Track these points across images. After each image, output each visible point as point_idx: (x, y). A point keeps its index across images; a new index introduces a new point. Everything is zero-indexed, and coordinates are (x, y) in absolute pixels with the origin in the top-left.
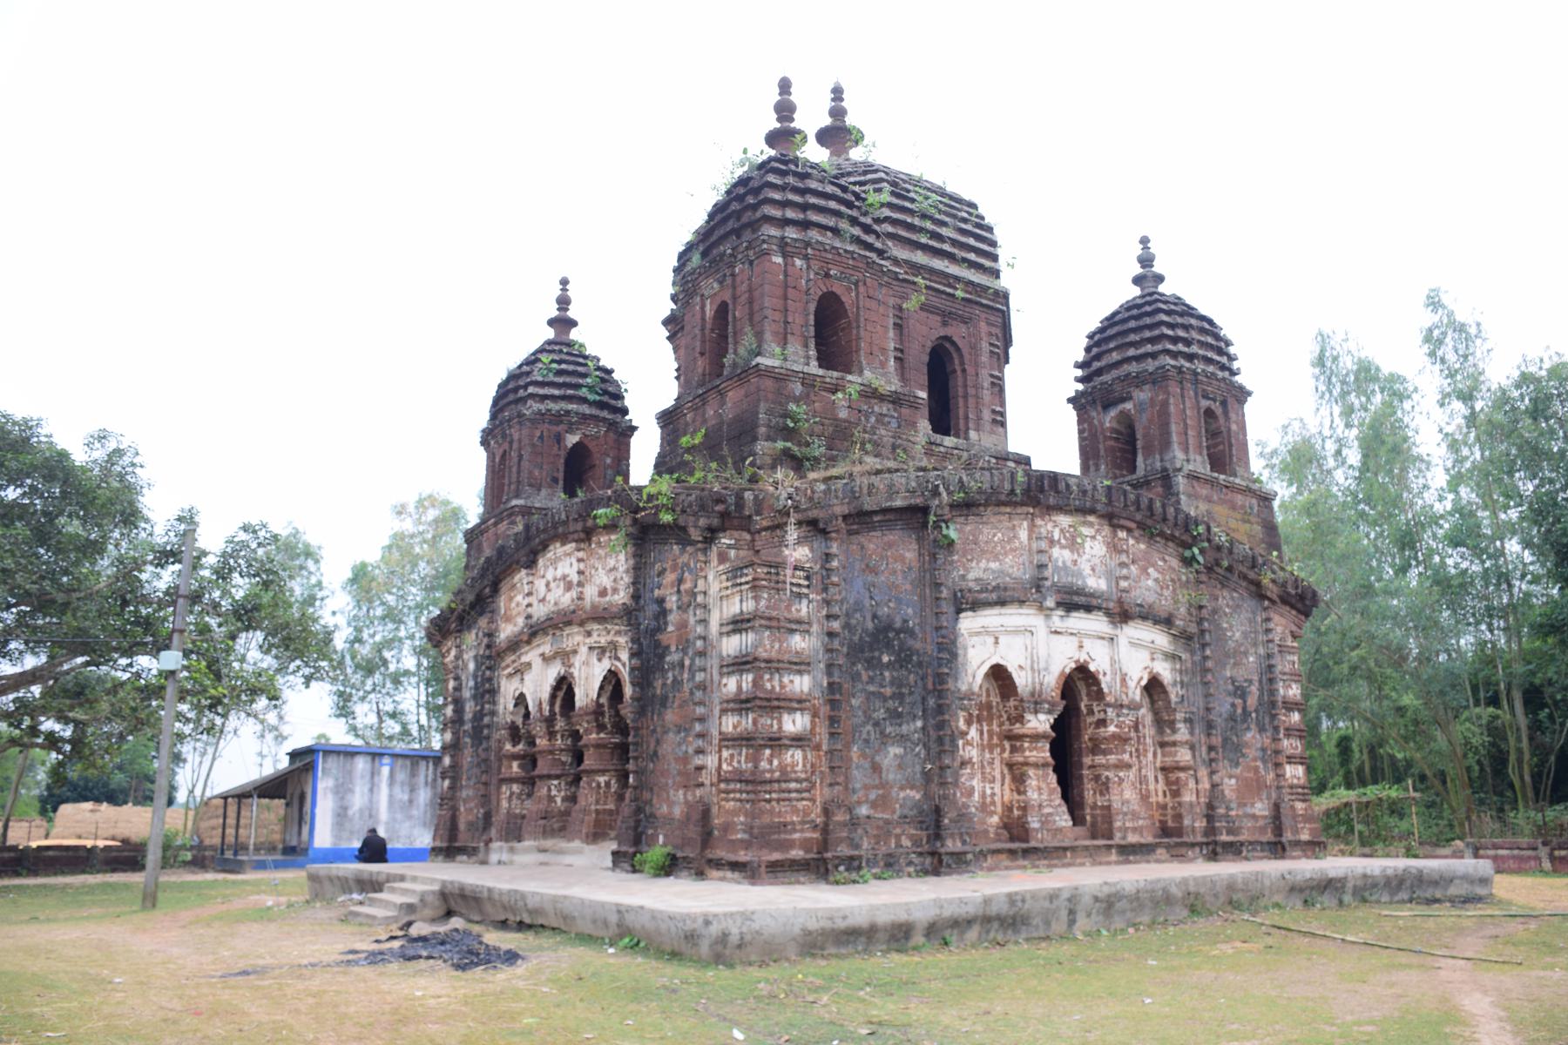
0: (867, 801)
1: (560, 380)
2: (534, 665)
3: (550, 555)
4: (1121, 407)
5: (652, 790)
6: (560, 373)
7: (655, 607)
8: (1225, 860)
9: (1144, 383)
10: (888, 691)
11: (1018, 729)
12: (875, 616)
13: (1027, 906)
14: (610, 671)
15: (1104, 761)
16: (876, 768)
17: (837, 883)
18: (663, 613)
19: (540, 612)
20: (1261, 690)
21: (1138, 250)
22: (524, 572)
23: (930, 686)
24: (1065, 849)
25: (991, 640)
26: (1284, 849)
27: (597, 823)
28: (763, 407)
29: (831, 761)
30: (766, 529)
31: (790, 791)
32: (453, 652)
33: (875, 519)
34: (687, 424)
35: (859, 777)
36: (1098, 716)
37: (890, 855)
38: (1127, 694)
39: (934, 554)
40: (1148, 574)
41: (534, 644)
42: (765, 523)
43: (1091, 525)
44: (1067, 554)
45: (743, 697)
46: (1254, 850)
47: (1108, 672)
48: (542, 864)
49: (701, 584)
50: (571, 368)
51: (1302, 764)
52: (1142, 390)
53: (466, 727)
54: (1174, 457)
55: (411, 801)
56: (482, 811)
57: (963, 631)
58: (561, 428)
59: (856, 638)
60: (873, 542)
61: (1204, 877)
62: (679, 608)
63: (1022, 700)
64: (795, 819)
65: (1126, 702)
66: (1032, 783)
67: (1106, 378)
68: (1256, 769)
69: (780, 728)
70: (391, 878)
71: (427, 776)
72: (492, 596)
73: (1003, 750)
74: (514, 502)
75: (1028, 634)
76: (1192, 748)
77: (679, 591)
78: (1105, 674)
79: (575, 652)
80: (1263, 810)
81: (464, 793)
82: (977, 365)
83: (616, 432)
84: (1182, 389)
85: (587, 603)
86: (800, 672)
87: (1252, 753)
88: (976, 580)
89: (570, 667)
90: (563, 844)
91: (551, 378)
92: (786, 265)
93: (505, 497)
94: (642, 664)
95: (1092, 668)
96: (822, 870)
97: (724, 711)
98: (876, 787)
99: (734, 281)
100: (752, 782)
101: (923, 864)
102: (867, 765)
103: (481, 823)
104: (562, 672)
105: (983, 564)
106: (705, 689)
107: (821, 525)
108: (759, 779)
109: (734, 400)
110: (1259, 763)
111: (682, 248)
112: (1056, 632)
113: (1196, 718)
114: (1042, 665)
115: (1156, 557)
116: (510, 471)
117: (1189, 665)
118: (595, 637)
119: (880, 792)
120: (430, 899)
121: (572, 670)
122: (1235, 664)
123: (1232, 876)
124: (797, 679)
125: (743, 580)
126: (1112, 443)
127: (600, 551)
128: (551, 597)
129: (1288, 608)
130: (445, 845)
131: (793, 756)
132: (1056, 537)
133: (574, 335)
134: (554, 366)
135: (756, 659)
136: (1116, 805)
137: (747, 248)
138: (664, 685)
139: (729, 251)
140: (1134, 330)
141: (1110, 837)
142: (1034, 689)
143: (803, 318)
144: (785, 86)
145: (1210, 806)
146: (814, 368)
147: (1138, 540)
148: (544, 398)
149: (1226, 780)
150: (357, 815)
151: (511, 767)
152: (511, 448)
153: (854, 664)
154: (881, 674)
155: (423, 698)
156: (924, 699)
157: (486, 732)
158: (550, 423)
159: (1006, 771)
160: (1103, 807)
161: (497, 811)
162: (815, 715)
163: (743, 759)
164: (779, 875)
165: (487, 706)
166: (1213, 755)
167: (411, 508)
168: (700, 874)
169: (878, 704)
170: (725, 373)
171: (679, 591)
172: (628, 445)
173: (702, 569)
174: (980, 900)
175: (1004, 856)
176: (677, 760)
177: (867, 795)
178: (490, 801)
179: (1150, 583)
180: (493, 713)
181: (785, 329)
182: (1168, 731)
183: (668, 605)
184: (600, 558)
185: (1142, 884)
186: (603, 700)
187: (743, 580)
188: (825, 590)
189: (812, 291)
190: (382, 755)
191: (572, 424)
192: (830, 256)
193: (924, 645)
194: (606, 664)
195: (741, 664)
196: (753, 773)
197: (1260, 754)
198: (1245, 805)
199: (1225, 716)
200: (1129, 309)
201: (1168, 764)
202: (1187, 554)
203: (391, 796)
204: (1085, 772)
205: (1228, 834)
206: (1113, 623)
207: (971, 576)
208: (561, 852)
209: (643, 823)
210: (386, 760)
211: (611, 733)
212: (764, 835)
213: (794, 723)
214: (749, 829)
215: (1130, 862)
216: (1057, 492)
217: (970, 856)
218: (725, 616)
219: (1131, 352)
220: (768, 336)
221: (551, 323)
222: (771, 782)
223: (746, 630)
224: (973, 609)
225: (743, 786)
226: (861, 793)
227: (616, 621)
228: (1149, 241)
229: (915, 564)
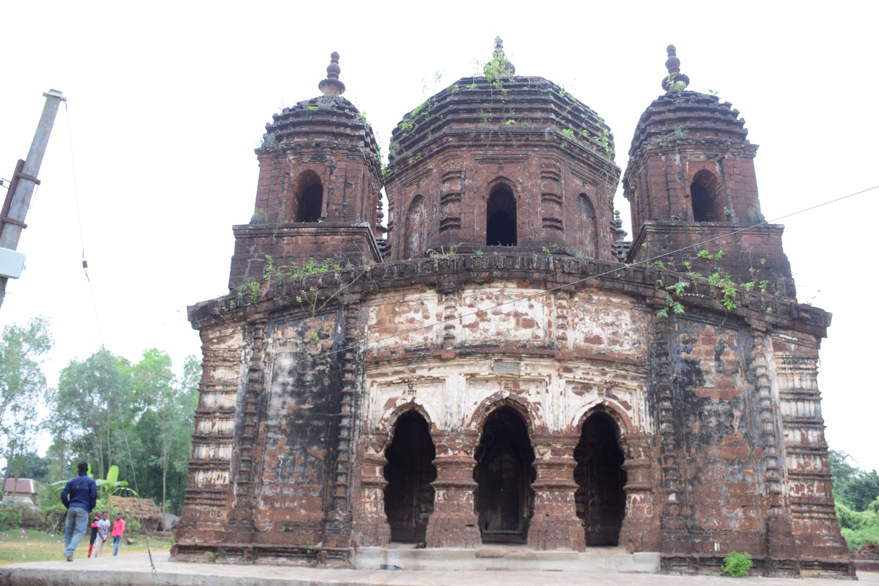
5: (692, 507)
14: (600, 406)
18: (693, 371)
48: (488, 569)
85: (570, 343)
97: (789, 454)
121: (523, 395)
125: (803, 366)
151: (374, 472)
157: (345, 434)
163: (815, 489)
176: (730, 485)
180: (356, 417)
184: (586, 311)
187: (803, 366)
194: (593, 399)
196: (828, 500)
208: (534, 558)
223: (809, 401)
225: (820, 509)
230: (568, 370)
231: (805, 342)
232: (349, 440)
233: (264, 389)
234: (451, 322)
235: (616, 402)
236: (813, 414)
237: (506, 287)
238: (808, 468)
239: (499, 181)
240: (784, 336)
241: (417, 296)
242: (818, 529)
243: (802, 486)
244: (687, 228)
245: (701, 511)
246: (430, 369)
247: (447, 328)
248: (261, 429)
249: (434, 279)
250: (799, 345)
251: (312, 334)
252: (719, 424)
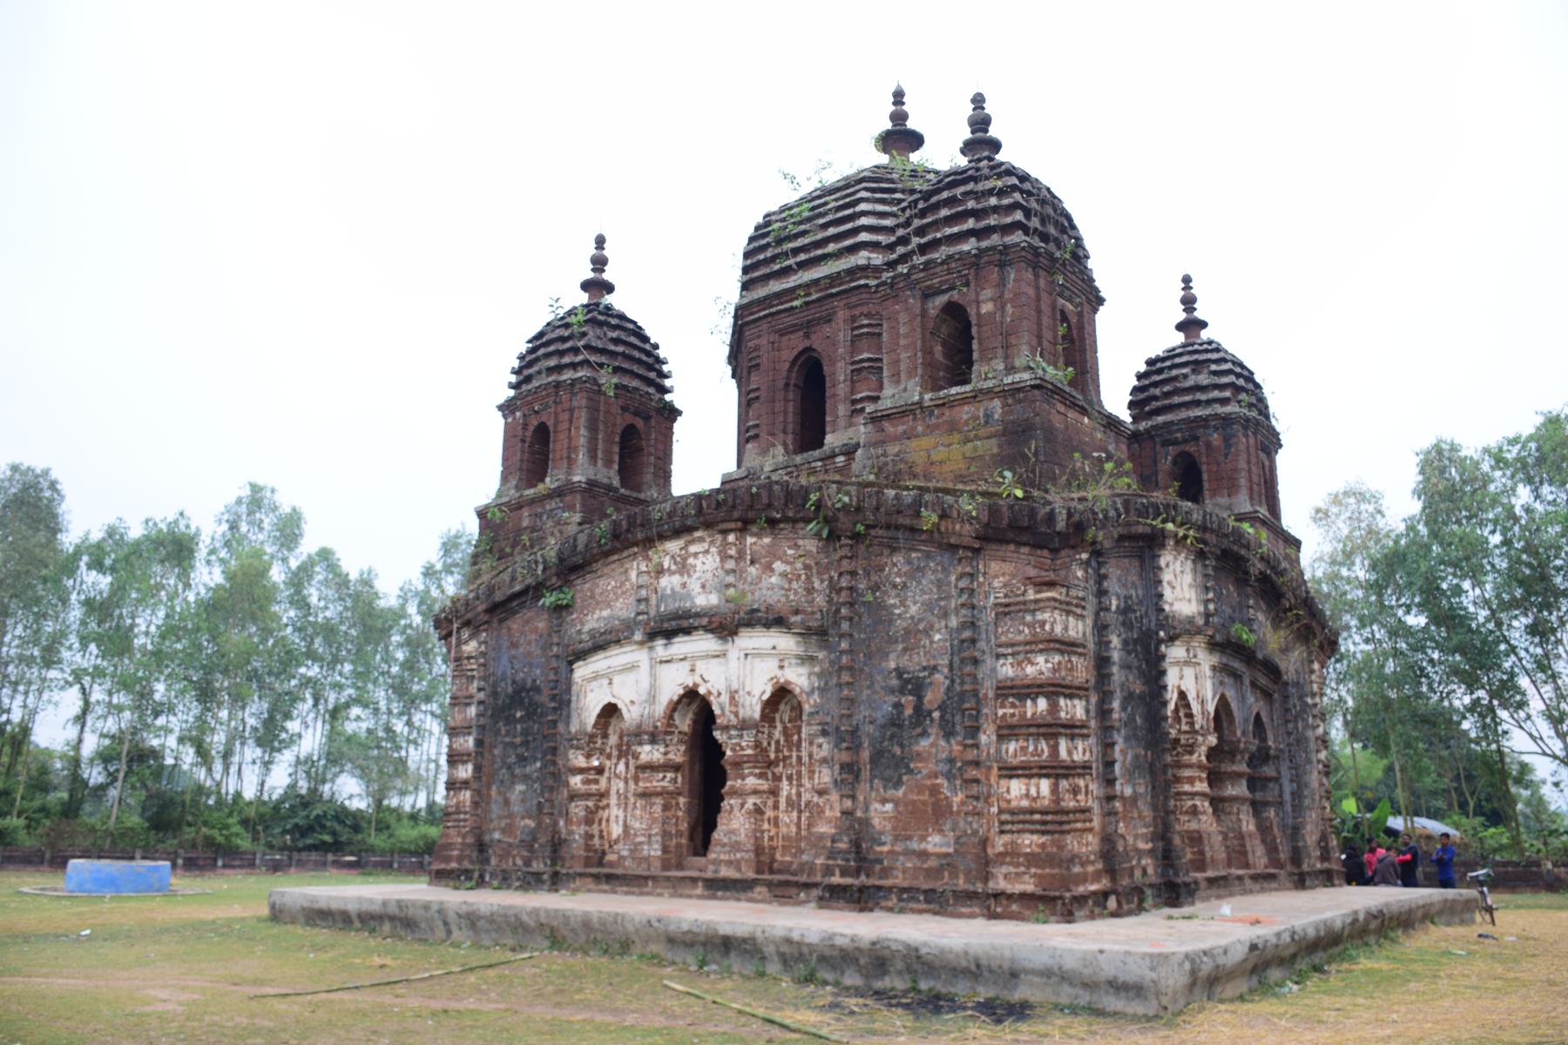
10: (518, 740)
12: (514, 682)
16: (507, 802)
24: (646, 878)
25: (606, 682)
33: (515, 604)
35: (496, 810)
38: (736, 714)
40: (772, 570)
43: (701, 540)
46: (911, 899)
47: (723, 692)
51: (1046, 776)
59: (500, 702)
60: (515, 624)
61: (556, 911)
68: (935, 790)
78: (719, 694)
80: (948, 845)
82: (833, 363)
95: (702, 691)
98: (506, 817)
102: (500, 799)
105: (596, 616)
112: (661, 662)
122: (905, 650)
123: (586, 914)
129: (1012, 547)
132: (666, 566)
144: (600, 242)
147: (759, 535)
149: (876, 806)
153: (497, 722)
169: (511, 751)
175: (589, 880)
179: (774, 580)
185: (495, 908)
193: (543, 698)
197: (943, 767)
198: (910, 838)
199: (881, 721)
205: (843, 875)
206: (720, 638)
215: (714, 897)
226: (496, 822)
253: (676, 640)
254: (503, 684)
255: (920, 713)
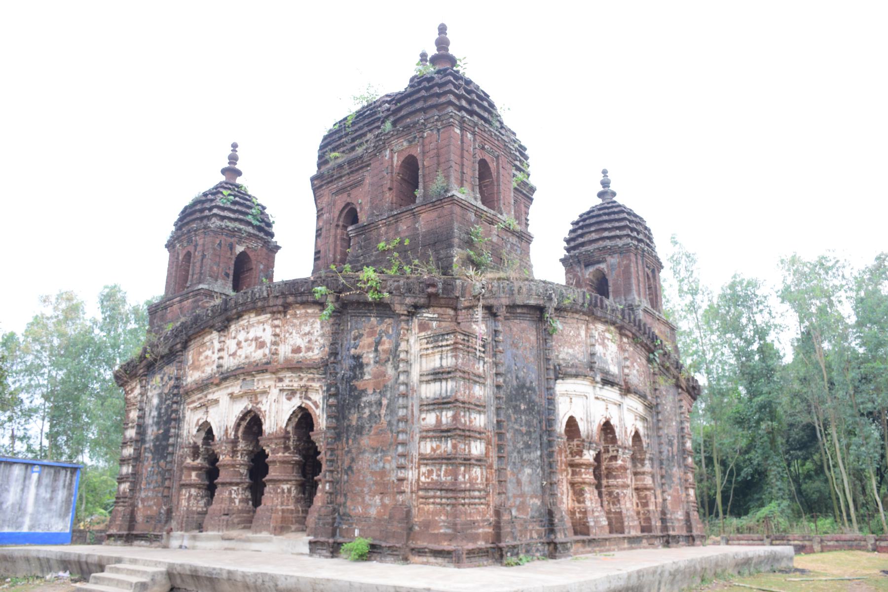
0: (514, 506)
1: (236, 208)
2: (221, 401)
3: (243, 322)
4: (597, 266)
5: (345, 495)
6: (234, 203)
7: (352, 362)
8: (673, 547)
9: (614, 253)
10: (524, 429)
11: (577, 459)
12: (517, 377)
13: (644, 579)
14: (300, 407)
15: (615, 483)
16: (519, 483)
17: (508, 565)
18: (358, 365)
19: (229, 363)
20: (678, 442)
21: (601, 177)
22: (215, 334)
23: (544, 428)
25: (568, 400)
26: (694, 540)
27: (284, 519)
28: (456, 225)
29: (499, 477)
30: (465, 308)
31: (475, 498)
32: (137, 391)
33: (519, 311)
34: (379, 235)
35: (511, 488)
36: (611, 454)
37: (528, 545)
39: (546, 339)
41: (221, 387)
42: (467, 304)
43: (611, 333)
44: (601, 347)
45: (443, 428)
48: (226, 549)
49: (403, 346)
50: (242, 201)
52: (612, 257)
53: (147, 446)
54: (634, 298)
55: (51, 499)
56: (164, 508)
57: (557, 393)
58: (232, 240)
62: (376, 362)
63: (583, 441)
64: (478, 518)
65: (627, 446)
66: (587, 495)
67: (590, 248)
69: (470, 451)
70: (110, 560)
71: (65, 481)
72: (181, 351)
73: (568, 474)
74: (201, 286)
75: (585, 398)
76: (653, 476)
77: (376, 350)
79: (265, 393)
81: (143, 495)
83: (268, 248)
84: (637, 259)
85: (281, 357)
86: (480, 412)
87: (676, 480)
88: (563, 359)
89: (257, 404)
90: (249, 534)
91: (229, 205)
92: (462, 135)
93: (188, 284)
94: (338, 402)
95: (612, 422)
96: (497, 556)
97: (423, 438)
98: (519, 496)
99: (423, 141)
100: (452, 491)
101: (544, 550)
102: (515, 481)
103: (163, 518)
104: (250, 407)
105: (566, 350)
106: (407, 421)
107: (495, 311)
108: (459, 489)
109: (425, 221)
110: (679, 487)
111: (326, 133)
112: (597, 398)
113: (655, 458)
114: (592, 419)
115: (637, 356)
116: (194, 266)
117: (651, 424)
118: (286, 382)
119: (521, 499)
120: (159, 578)
121: (260, 406)
124: (477, 416)
125: (444, 343)
126: (589, 288)
127: (295, 321)
128: (242, 353)
129: (687, 394)
130: (125, 533)
131: (476, 472)
133: (239, 181)
134: (232, 197)
135: (457, 400)
136: (624, 511)
137: (437, 120)
138: (359, 418)
139: (422, 121)
140: (606, 221)
141: (623, 532)
142: (588, 433)
143: (472, 171)
145: (663, 513)
146: (479, 204)
148: (223, 218)
150: (10, 508)
151: (191, 476)
152: (196, 250)
154: (521, 417)
155: (47, 429)
156: (541, 436)
157: (170, 449)
158: (226, 235)
159: (569, 488)
160: (615, 513)
161: (177, 508)
162: (488, 443)
164: (472, 559)
165: (173, 430)
166: (663, 481)
167: (53, 300)
168: (406, 560)
169: (520, 438)
170: (417, 201)
171: (376, 350)
172: (274, 258)
173: (404, 335)
174: (626, 576)
175: (579, 545)
176: (373, 473)
177: (514, 502)
178: (171, 501)
180: (177, 436)
181: (462, 177)
182: (639, 465)
183: (364, 360)
184: (294, 325)
186: (289, 429)
187: (444, 343)
188: (495, 355)
189: (477, 155)
190: (34, 465)
191: (241, 238)
192: (486, 136)
193: (539, 399)
194: (296, 402)
195: (440, 404)
200: (600, 209)
201: (640, 486)
202: (651, 356)
203: (37, 495)
204: (603, 490)
206: (621, 394)
207: (561, 356)
208: (248, 540)
209: (337, 520)
210: (36, 469)
211: (293, 453)
212: (458, 531)
213: (477, 448)
214: (454, 525)
216: (602, 308)
217: (569, 545)
218: (424, 368)
219: (606, 234)
220: (452, 179)
221: (224, 171)
222: (465, 491)
223: (446, 379)
224: (563, 379)
225: (444, 494)
226: (512, 500)
227: (312, 371)
228: (607, 172)
229: (535, 344)
230: (281, 380)
231: (444, 316)
232: (173, 454)
233: (144, 422)
234: (221, 354)
235: (310, 403)
236: (449, 394)
237: (250, 317)
238: (438, 452)
239: (349, 207)
240: (427, 314)
241: (209, 337)
242: (437, 516)
243: (432, 470)
244: (376, 224)
245: (351, 499)
246: (214, 393)
247: (219, 358)
248: (142, 451)
249: (211, 323)
250: (440, 321)
251: (166, 378)
252: (371, 414)
253: (606, 387)
254: (509, 375)
255: (673, 457)
